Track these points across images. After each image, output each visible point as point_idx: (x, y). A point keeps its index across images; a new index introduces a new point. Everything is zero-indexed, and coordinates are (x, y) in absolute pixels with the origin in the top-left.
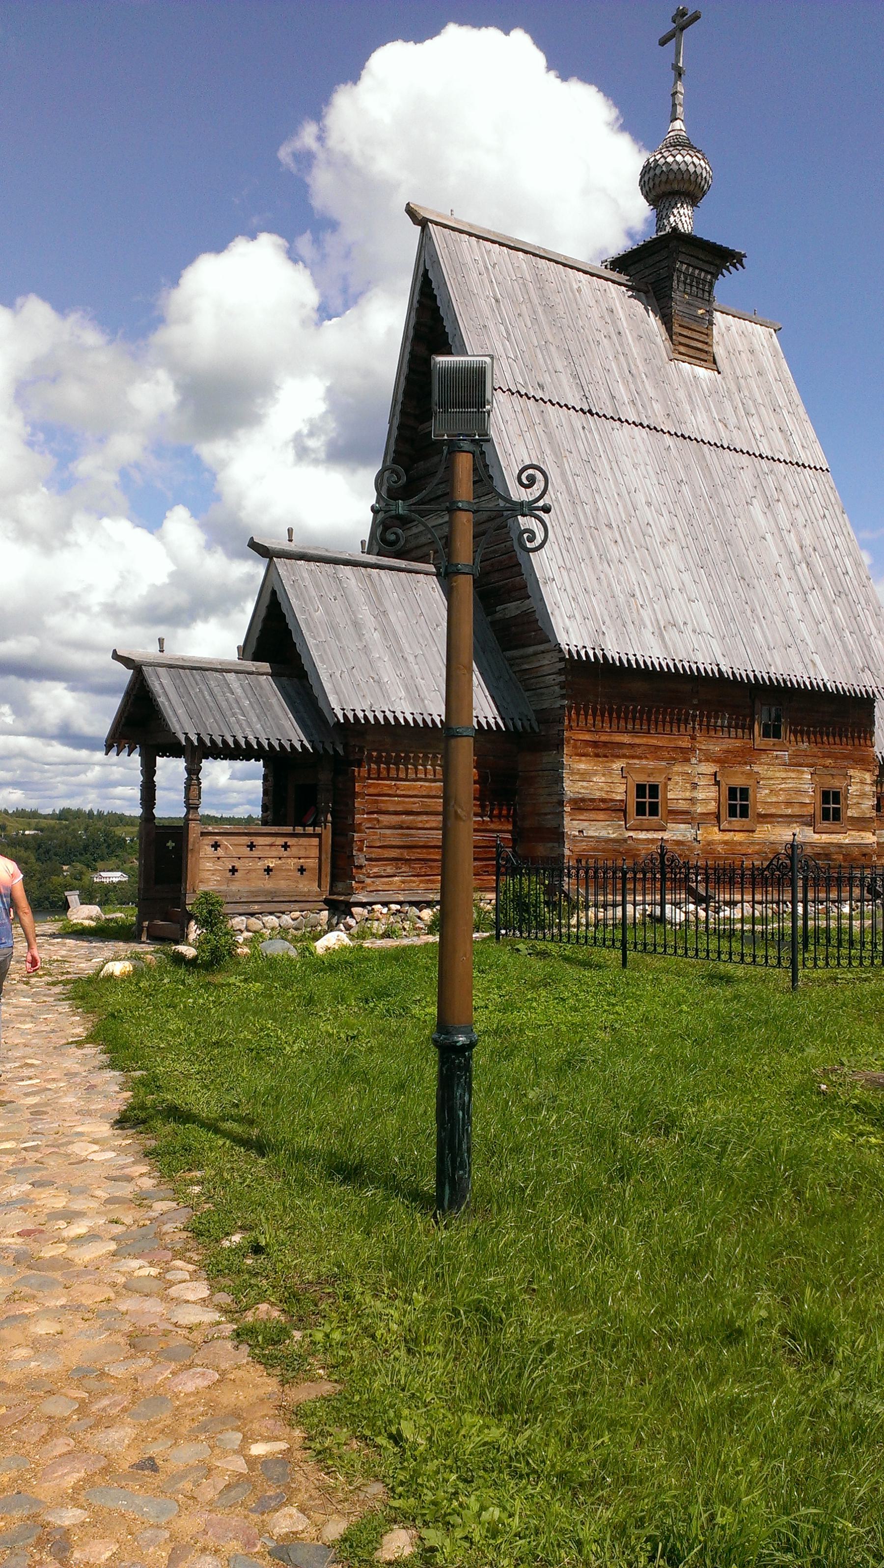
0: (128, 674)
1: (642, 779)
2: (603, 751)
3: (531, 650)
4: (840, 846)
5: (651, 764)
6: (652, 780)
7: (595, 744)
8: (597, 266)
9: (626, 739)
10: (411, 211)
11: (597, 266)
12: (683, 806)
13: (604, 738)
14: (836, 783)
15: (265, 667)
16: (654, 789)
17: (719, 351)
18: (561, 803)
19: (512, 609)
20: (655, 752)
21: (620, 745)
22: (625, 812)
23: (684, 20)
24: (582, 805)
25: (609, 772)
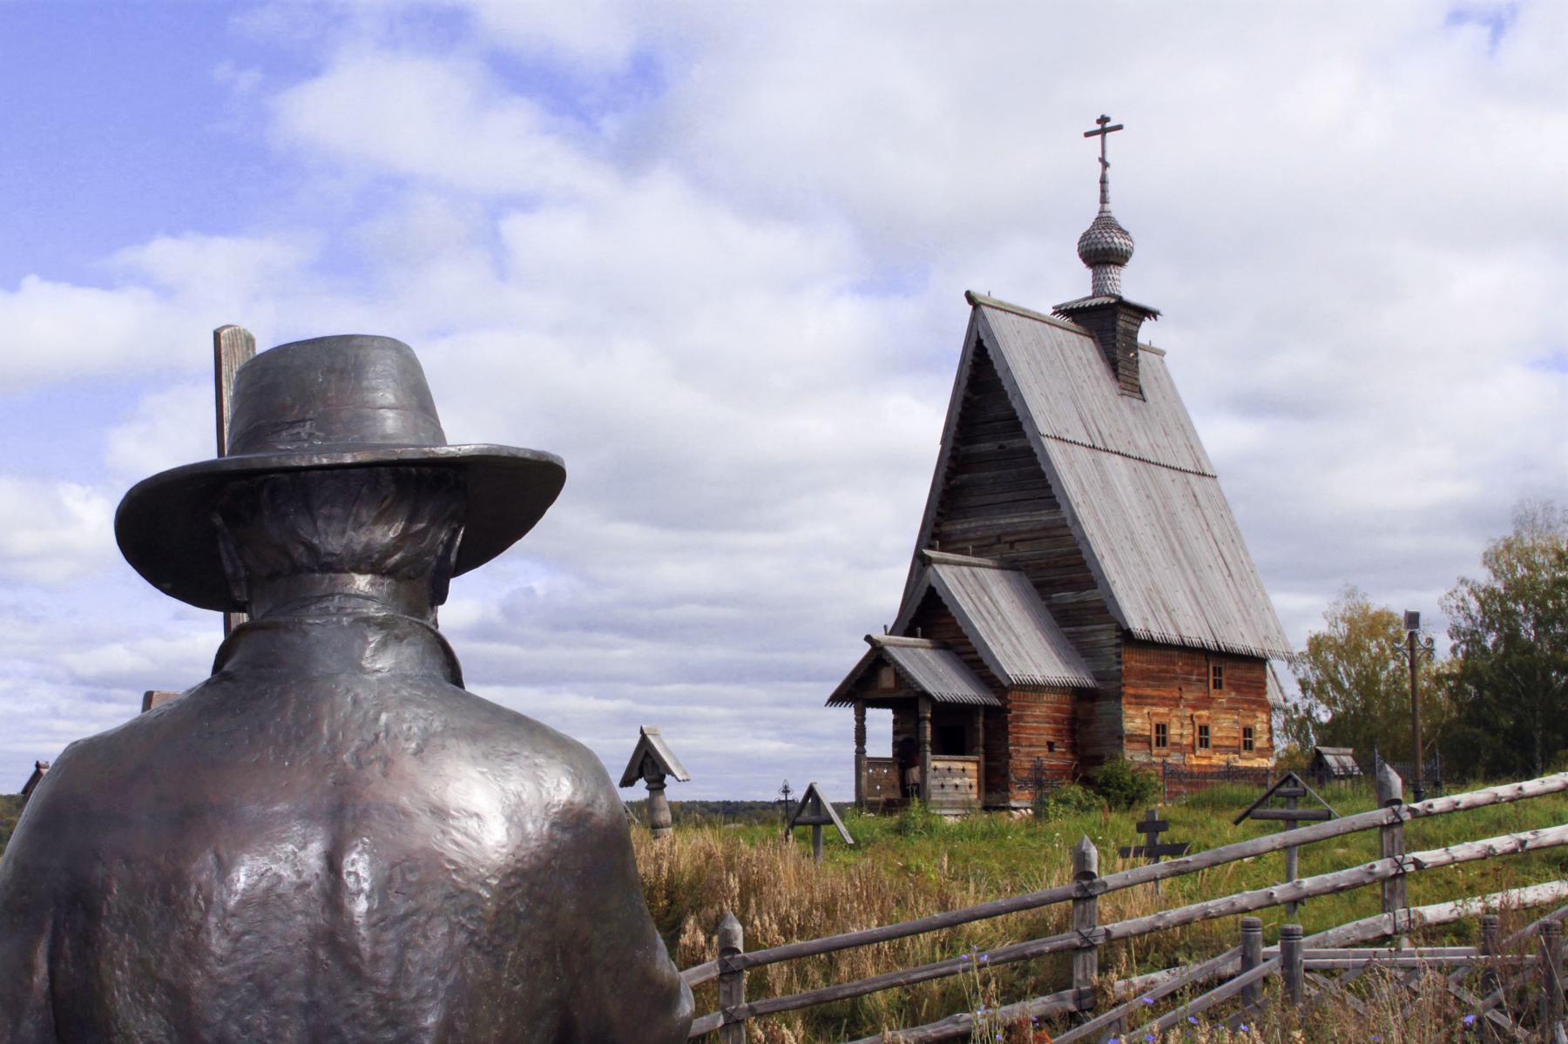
0: (868, 647)
1: (1156, 720)
2: (1140, 701)
3: (1089, 628)
4: (1252, 769)
5: (1161, 710)
6: (1164, 720)
7: (1136, 696)
8: (1047, 311)
9: (1148, 691)
10: (970, 297)
11: (1047, 311)
12: (1176, 739)
13: (1140, 692)
14: (1249, 722)
15: (925, 642)
16: (1164, 727)
17: (1142, 381)
18: (1121, 738)
19: (1068, 597)
20: (1162, 701)
21: (1147, 697)
22: (1150, 744)
23: (1104, 127)
24: (1133, 738)
25: (1142, 717)
